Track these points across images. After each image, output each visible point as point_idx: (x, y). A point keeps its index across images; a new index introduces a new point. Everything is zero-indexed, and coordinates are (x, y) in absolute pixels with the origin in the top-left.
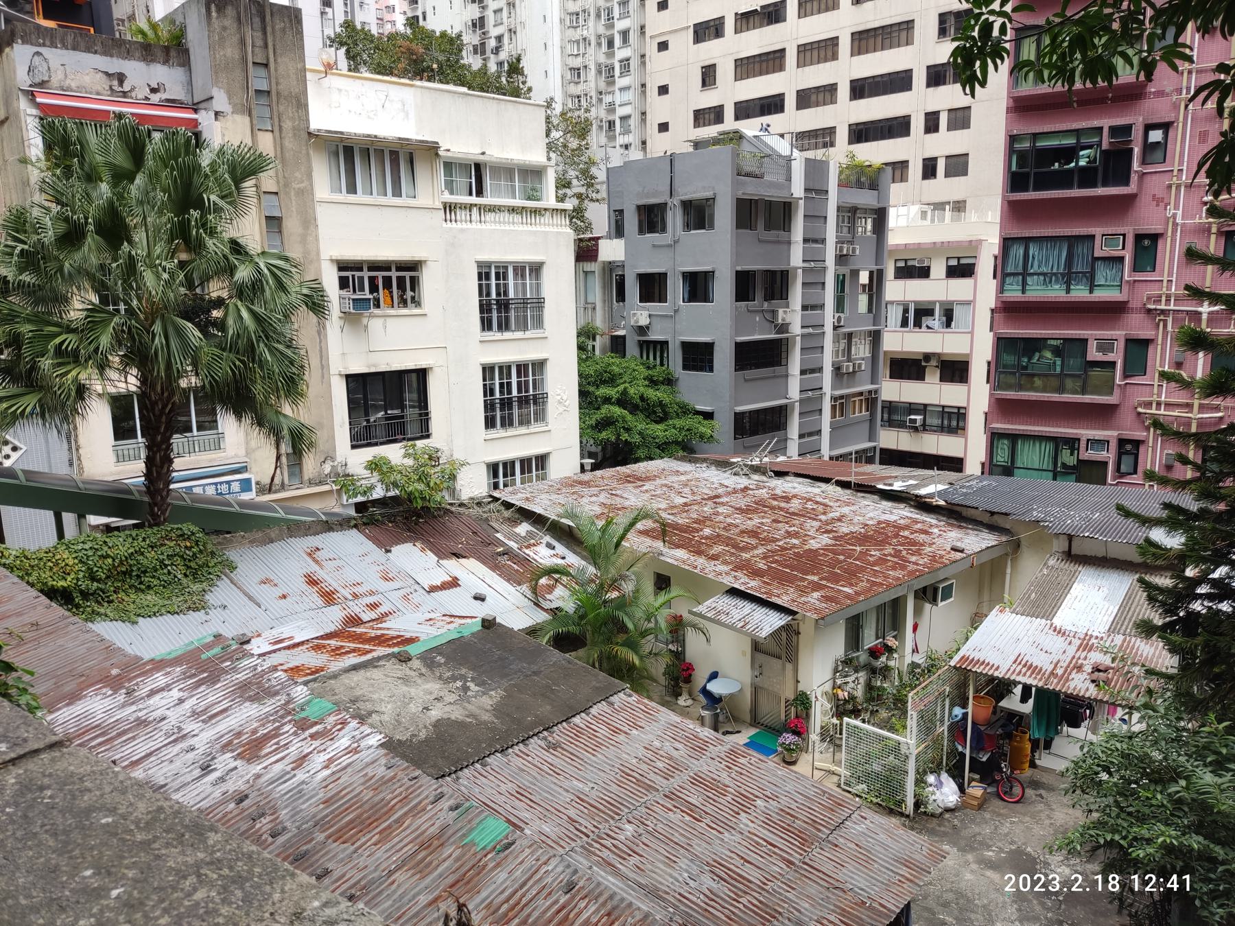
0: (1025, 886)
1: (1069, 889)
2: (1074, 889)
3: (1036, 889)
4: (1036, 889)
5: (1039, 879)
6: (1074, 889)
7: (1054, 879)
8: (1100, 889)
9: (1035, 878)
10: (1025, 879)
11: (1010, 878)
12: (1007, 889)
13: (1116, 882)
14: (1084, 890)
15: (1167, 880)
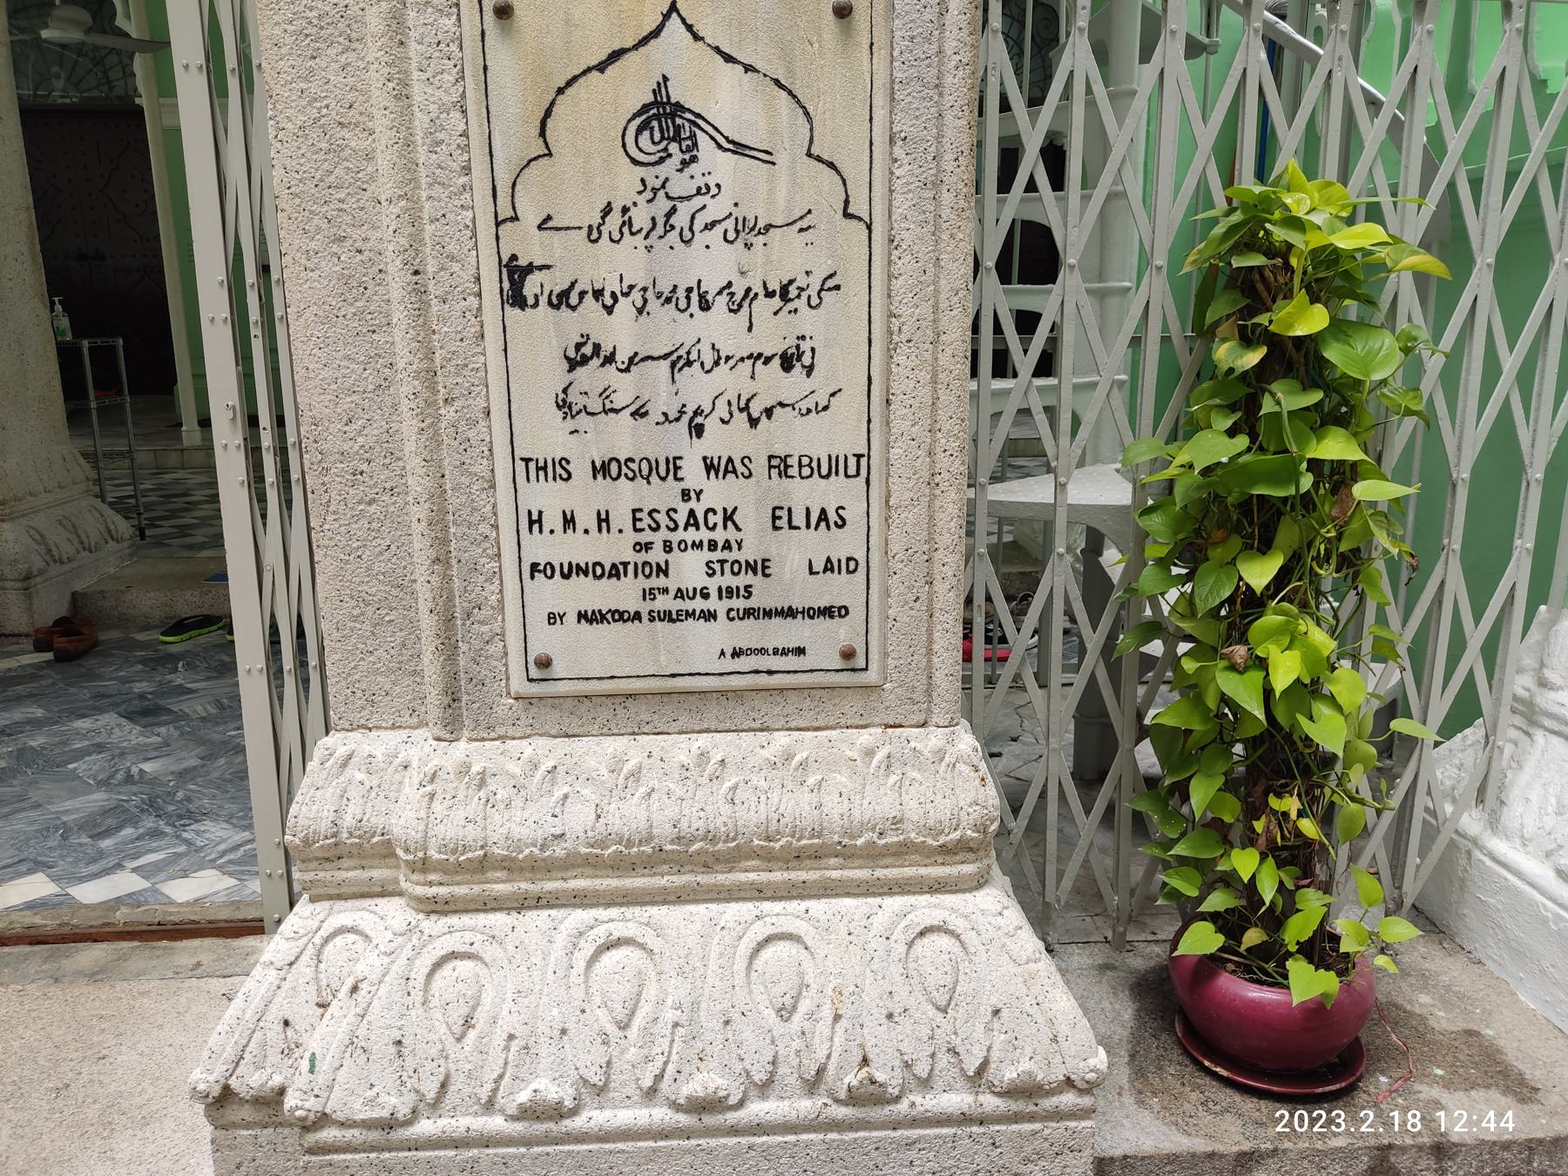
4: (1316, 1129)
5: (1320, 1116)
9: (1314, 1115)
11: (1282, 1116)
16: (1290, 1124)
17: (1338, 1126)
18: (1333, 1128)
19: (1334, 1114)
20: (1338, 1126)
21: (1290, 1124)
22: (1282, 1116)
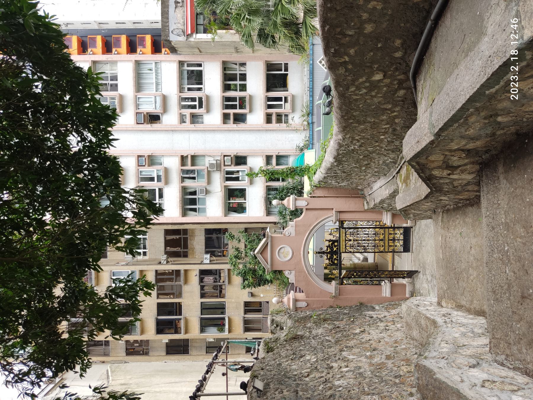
0: (516, 91)
2: (517, 70)
3: (517, 86)
4: (517, 86)
5: (512, 85)
6: (517, 70)
7: (513, 78)
8: (517, 58)
9: (512, 86)
10: (513, 91)
12: (517, 99)
13: (514, 53)
16: (515, 95)
17: (516, 78)
18: (517, 80)
19: (512, 80)
20: (516, 78)
21: (515, 95)
22: (513, 97)
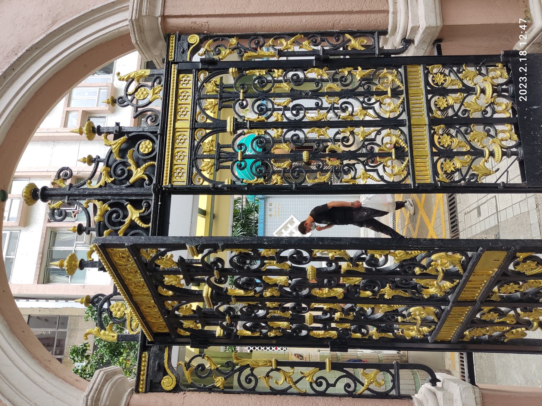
0: (524, 92)
1: (526, 73)
2: (526, 71)
3: (526, 87)
4: (526, 87)
5: (521, 86)
6: (526, 71)
7: (521, 79)
8: (526, 59)
9: (521, 88)
10: (521, 92)
11: (521, 99)
12: (526, 100)
14: (526, 66)
15: (522, 30)
16: (524, 96)
17: (525, 79)
18: (525, 81)
19: (521, 81)
20: (525, 79)
21: (524, 96)
22: (521, 99)
